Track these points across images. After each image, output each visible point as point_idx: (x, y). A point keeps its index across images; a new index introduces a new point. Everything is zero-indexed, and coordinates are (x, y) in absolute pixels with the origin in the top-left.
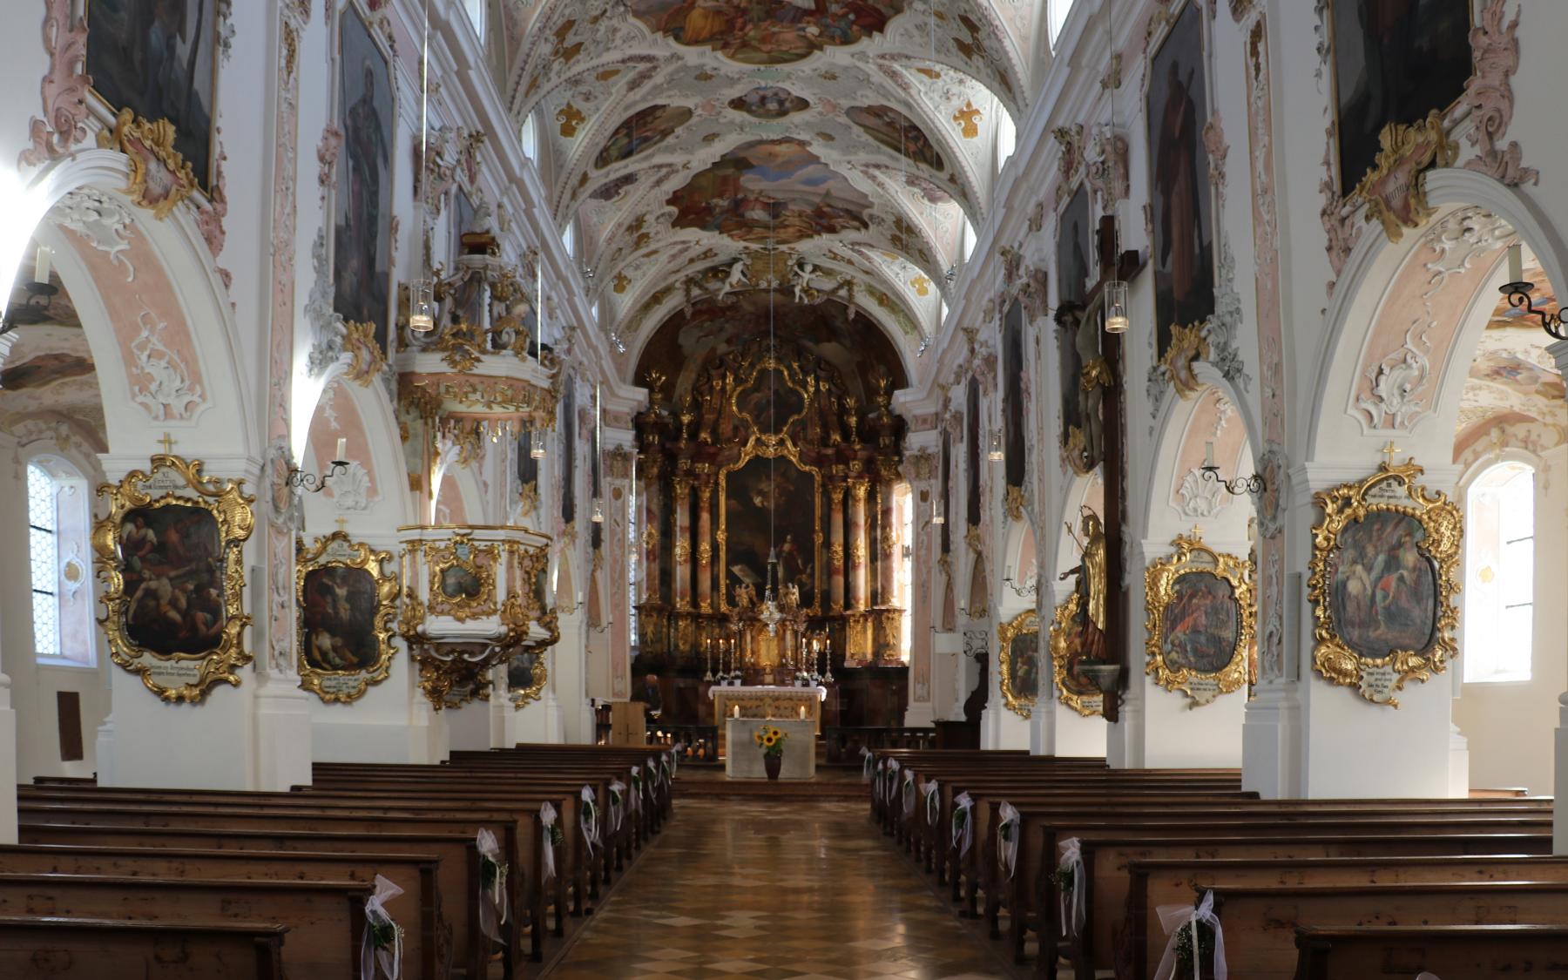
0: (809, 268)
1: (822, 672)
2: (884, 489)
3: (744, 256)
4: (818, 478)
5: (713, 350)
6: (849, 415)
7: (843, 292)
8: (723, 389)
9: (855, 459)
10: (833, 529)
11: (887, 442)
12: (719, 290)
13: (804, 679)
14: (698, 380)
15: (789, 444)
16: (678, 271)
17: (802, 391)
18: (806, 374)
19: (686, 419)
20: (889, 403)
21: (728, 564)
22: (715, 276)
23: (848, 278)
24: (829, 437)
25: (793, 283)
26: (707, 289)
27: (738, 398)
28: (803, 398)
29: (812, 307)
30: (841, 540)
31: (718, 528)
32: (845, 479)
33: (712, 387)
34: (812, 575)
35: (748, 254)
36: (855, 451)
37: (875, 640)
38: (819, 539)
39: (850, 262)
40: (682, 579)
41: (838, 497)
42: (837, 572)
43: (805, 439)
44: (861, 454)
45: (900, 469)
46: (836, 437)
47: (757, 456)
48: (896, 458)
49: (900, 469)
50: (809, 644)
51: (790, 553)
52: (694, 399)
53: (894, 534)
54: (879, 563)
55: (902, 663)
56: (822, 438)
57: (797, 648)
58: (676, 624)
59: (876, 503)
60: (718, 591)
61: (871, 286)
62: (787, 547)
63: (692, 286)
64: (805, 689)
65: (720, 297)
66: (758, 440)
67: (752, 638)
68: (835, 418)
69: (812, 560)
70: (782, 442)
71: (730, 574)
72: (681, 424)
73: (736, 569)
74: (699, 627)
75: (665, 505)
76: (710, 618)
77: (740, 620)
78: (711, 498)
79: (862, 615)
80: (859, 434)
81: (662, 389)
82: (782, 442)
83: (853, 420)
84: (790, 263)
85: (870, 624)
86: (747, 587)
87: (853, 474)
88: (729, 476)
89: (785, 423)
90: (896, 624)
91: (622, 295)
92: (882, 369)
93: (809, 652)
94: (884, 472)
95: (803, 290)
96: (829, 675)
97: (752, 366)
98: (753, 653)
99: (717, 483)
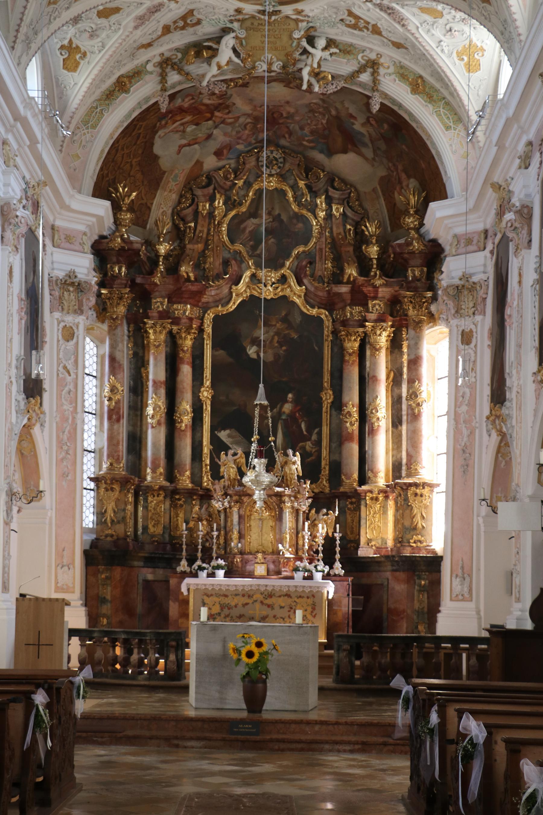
0: (321, 43)
1: (329, 561)
2: (411, 332)
3: (236, 25)
4: (328, 324)
5: (199, 164)
6: (368, 243)
7: (365, 77)
8: (211, 215)
9: (375, 298)
10: (345, 384)
11: (417, 273)
12: (203, 76)
13: (306, 570)
14: (179, 202)
15: (292, 281)
16: (149, 45)
17: (310, 216)
18: (314, 194)
19: (163, 249)
20: (422, 225)
21: (214, 428)
22: (198, 54)
23: (373, 56)
24: (342, 270)
25: (299, 66)
26: (188, 74)
27: (228, 225)
28: (312, 226)
29: (324, 97)
30: (356, 399)
31: (202, 384)
32: (362, 323)
33: (196, 213)
34: (318, 443)
35: (242, 21)
36: (375, 287)
37: (396, 522)
38: (327, 397)
39: (376, 31)
40: (154, 445)
41: (353, 345)
42: (350, 438)
43: (312, 275)
44: (384, 292)
45: (433, 308)
46: (352, 272)
47: (252, 296)
48: (429, 294)
49: (433, 308)
50: (313, 526)
51: (292, 415)
52: (175, 226)
53: (424, 388)
54: (404, 427)
55: (434, 552)
56: (334, 274)
57: (297, 532)
58: (146, 500)
59: (402, 353)
60: (201, 461)
61: (402, 67)
62: (287, 408)
63: (168, 69)
64: (308, 583)
65: (205, 83)
66: (253, 276)
67: (240, 517)
68: (351, 249)
69: (319, 424)
70: (283, 279)
71: (215, 441)
72: (158, 256)
73: (223, 435)
74: (174, 505)
75: (135, 354)
76: (190, 494)
77: (226, 495)
78: (193, 347)
79: (381, 491)
80: (381, 266)
81: (131, 209)
82: (283, 279)
83: (373, 251)
84: (296, 35)
85: (391, 503)
86: (235, 454)
87: (372, 316)
88: (217, 319)
89: (288, 257)
90: (426, 502)
91: (75, 74)
92: (413, 183)
93: (313, 537)
94: (411, 312)
95: (316, 74)
96: (338, 565)
97: (248, 185)
98: (241, 536)
99: (201, 330)
